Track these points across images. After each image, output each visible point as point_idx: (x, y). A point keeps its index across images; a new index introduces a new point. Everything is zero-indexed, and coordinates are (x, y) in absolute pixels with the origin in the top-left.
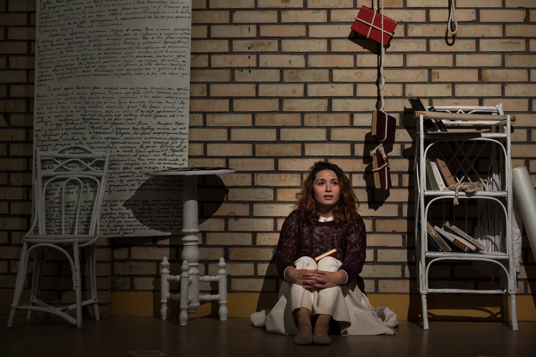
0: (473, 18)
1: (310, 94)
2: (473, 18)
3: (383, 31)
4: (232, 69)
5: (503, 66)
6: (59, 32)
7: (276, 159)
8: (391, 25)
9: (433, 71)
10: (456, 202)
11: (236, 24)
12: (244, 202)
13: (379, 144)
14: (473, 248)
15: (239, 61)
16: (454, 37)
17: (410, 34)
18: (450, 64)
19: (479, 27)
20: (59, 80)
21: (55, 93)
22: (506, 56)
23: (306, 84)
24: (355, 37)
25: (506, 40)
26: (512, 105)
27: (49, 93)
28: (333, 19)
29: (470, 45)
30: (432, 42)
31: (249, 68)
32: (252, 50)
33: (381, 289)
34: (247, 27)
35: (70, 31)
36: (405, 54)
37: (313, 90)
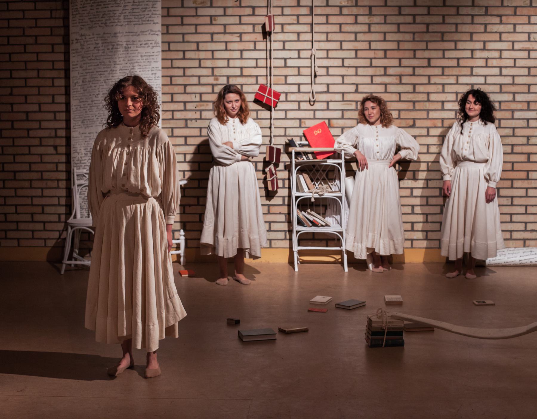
0: (326, 90)
2: (326, 90)
3: (273, 99)
4: (186, 120)
5: (342, 118)
6: (84, 100)
8: (277, 95)
9: (302, 120)
10: (313, 200)
11: (188, 93)
13: (270, 164)
14: (324, 224)
15: (189, 115)
17: (289, 99)
18: (312, 117)
19: (329, 95)
20: (85, 128)
21: (83, 135)
22: (345, 112)
24: (256, 101)
27: (80, 136)
29: (324, 106)
30: (302, 104)
31: (196, 119)
32: (197, 109)
34: (194, 95)
35: (91, 100)
36: (286, 111)
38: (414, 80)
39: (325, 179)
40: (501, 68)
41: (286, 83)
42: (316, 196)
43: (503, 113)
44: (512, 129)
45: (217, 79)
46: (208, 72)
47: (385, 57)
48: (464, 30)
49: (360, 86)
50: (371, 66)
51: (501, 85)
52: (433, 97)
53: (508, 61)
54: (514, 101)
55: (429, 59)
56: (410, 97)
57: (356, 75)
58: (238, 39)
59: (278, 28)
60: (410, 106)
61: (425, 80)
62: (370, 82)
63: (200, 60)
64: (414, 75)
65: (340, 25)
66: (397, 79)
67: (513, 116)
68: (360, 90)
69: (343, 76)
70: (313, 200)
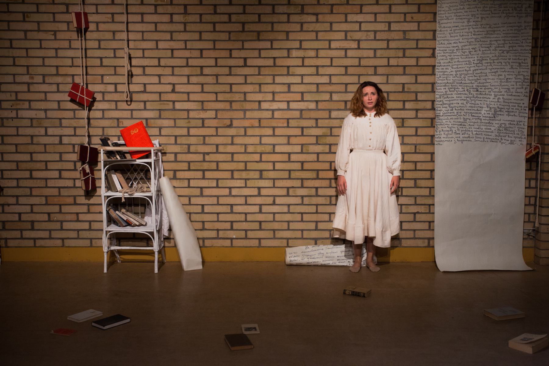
0: (142, 89)
1: (49, 133)
2: (142, 89)
3: (85, 97)
7: (31, 171)
10: (123, 200)
12: (13, 196)
14: (138, 224)
16: (131, 101)
18: (130, 117)
23: (46, 128)
24: (73, 101)
26: (164, 140)
28: (60, 90)
31: (12, 118)
32: (13, 107)
33: (94, 244)
37: (50, 131)
38: (231, 80)
39: (143, 179)
40: (317, 67)
41: (102, 83)
42: (127, 195)
43: (320, 112)
44: (329, 129)
45: (32, 78)
46: (23, 70)
47: (201, 57)
48: (280, 29)
49: (177, 86)
50: (187, 66)
52: (250, 97)
53: (324, 60)
54: (331, 100)
55: (245, 59)
56: (228, 97)
57: (173, 75)
58: (53, 37)
59: (92, 27)
60: (227, 106)
61: (241, 80)
62: (186, 82)
63: (14, 58)
64: (230, 75)
65: (156, 23)
67: (330, 115)
68: (176, 90)
69: (159, 76)
70: (123, 200)
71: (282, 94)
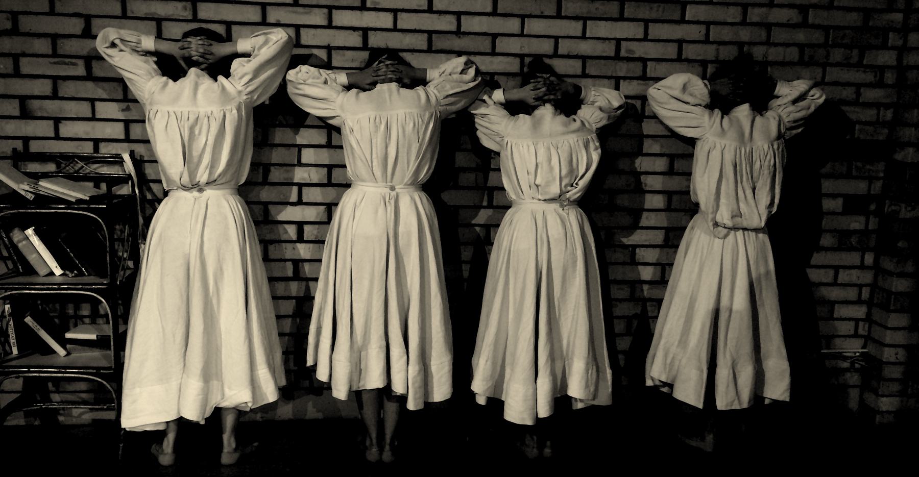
5: (55, 96)
19: (17, 39)
25: (56, 60)
51: (430, 33)
66: (185, 8)
71: (349, 54)
